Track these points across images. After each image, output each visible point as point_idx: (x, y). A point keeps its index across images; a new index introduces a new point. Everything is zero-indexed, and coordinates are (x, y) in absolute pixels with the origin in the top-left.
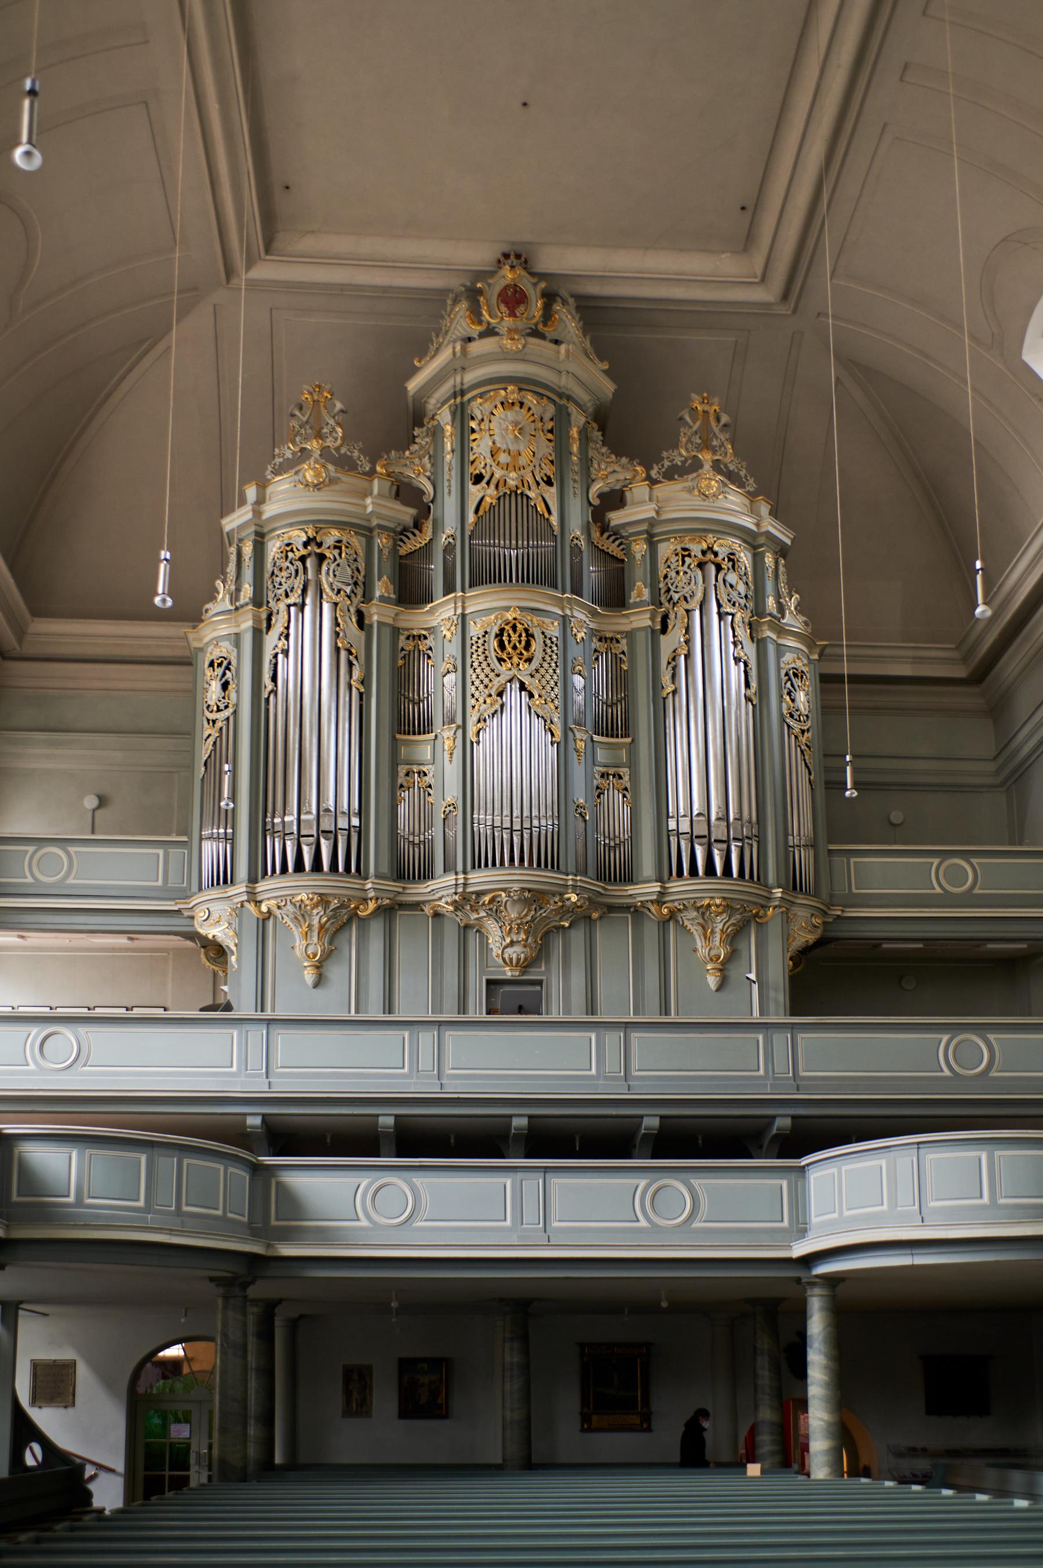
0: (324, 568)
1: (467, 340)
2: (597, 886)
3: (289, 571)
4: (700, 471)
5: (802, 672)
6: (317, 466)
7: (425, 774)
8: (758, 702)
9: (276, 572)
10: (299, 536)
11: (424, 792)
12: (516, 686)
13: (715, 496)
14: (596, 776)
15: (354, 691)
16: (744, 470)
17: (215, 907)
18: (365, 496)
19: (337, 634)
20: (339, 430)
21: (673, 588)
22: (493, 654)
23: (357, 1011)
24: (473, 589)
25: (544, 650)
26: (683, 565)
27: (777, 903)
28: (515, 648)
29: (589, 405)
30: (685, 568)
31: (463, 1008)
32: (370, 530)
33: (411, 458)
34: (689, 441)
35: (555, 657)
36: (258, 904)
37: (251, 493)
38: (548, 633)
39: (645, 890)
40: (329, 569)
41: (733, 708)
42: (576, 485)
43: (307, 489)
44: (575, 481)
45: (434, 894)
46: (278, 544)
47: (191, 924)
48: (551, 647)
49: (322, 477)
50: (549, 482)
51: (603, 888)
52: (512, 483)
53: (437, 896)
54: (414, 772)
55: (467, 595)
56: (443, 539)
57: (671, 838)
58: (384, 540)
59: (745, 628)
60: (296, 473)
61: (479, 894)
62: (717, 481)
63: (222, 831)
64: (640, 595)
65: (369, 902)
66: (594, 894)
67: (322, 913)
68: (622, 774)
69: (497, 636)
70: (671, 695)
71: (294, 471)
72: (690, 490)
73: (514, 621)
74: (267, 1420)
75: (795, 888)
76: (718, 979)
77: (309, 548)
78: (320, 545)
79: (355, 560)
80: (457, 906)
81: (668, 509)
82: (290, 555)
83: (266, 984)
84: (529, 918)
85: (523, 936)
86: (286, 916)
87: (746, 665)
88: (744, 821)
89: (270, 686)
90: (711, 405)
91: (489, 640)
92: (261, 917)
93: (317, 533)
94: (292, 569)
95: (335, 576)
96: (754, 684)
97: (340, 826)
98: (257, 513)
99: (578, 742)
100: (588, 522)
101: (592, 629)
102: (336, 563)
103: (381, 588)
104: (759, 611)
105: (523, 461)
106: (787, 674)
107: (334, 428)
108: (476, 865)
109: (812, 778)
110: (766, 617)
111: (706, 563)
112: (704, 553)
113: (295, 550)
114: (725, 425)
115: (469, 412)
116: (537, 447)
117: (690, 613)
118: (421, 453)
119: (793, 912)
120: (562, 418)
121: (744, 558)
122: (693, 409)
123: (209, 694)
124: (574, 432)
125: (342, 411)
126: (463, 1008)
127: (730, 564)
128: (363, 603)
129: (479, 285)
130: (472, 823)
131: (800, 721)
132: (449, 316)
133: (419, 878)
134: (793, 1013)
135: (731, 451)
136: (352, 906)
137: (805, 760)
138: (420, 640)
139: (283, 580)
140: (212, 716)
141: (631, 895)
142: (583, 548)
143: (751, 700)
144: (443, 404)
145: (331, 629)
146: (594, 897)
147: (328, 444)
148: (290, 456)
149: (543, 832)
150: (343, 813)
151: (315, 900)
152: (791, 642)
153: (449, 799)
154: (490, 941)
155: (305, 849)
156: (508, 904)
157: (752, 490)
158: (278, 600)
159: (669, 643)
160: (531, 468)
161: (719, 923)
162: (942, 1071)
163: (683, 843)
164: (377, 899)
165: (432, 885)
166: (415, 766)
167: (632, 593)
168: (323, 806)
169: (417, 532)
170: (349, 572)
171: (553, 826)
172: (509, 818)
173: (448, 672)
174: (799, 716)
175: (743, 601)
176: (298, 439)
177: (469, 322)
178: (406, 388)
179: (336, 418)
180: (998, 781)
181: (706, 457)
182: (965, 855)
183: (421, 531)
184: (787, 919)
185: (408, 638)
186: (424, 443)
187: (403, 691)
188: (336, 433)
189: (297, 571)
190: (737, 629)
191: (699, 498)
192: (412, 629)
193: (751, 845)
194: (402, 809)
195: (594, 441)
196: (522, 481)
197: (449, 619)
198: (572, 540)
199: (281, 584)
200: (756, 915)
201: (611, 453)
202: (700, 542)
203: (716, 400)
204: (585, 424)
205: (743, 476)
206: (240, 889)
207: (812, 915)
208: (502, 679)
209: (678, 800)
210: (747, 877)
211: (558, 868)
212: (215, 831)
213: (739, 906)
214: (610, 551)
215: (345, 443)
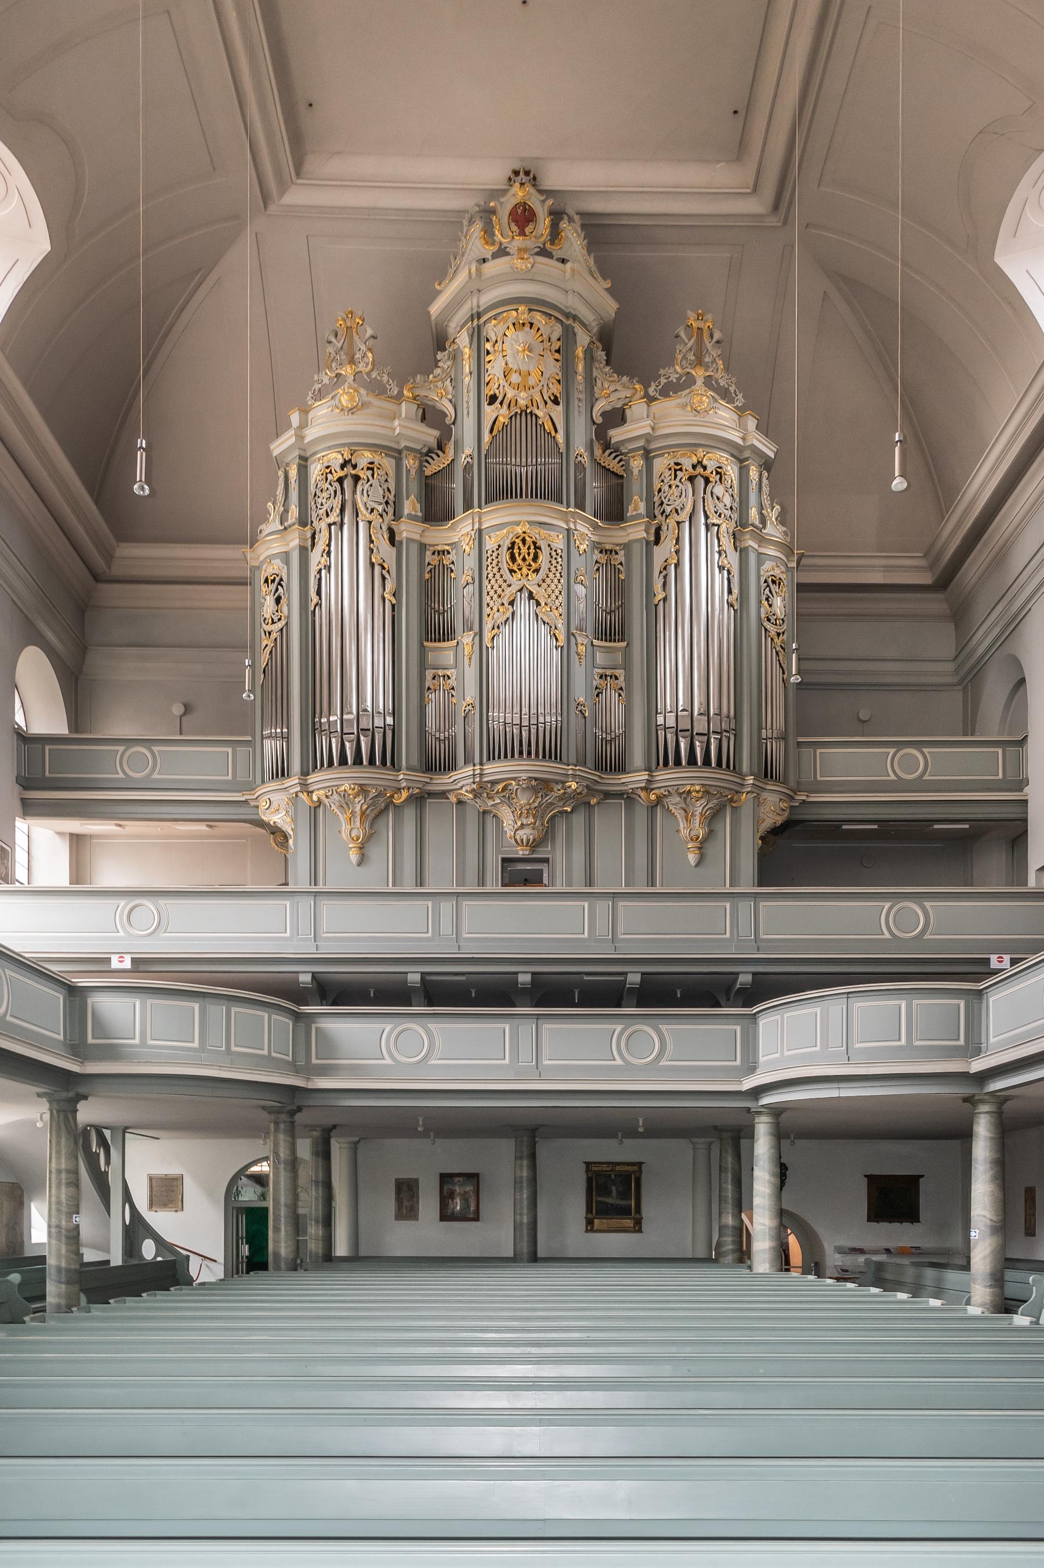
0: (359, 488)
1: (482, 261)
2: (594, 775)
3: (328, 492)
4: (693, 387)
5: (780, 579)
6: (351, 391)
7: (449, 678)
8: (739, 608)
9: (317, 493)
10: (336, 459)
11: (448, 693)
12: (525, 595)
13: (706, 411)
14: (596, 678)
15: (387, 601)
16: (734, 386)
17: (276, 797)
18: (394, 419)
19: (372, 551)
20: (370, 355)
21: (666, 501)
22: (505, 566)
23: (394, 885)
24: (488, 505)
25: (550, 562)
26: (675, 479)
27: (749, 789)
28: (524, 559)
29: (594, 324)
30: (677, 482)
31: (482, 882)
32: (400, 452)
33: (435, 382)
34: (684, 357)
35: (559, 568)
36: (310, 794)
37: (295, 418)
38: (554, 546)
39: (635, 779)
40: (363, 490)
41: (717, 613)
42: (580, 404)
43: (342, 412)
44: (580, 400)
45: (456, 784)
46: (319, 467)
47: (256, 812)
48: (556, 559)
49: (356, 401)
50: (556, 402)
51: (600, 776)
52: (522, 403)
53: (460, 785)
54: (440, 677)
55: (483, 511)
56: (463, 460)
57: (659, 732)
58: (412, 462)
59: (729, 537)
60: (333, 398)
61: (494, 783)
62: (708, 397)
63: (279, 730)
64: (635, 510)
65: (402, 791)
66: (592, 783)
67: (363, 801)
68: (618, 675)
69: (509, 549)
70: (662, 602)
71: (331, 396)
72: (684, 406)
73: (524, 535)
74: (327, 1221)
75: (766, 776)
76: (697, 856)
77: (345, 469)
78: (355, 467)
79: (386, 481)
80: (476, 795)
81: (664, 424)
82: (329, 476)
83: (318, 864)
84: (536, 804)
85: (531, 820)
86: (333, 803)
87: (729, 573)
88: (723, 716)
89: (315, 599)
90: (705, 322)
91: (502, 553)
92: (313, 806)
93: (352, 455)
94: (332, 490)
95: (368, 496)
96: (736, 591)
97: (376, 725)
98: (300, 437)
99: (579, 645)
100: (592, 440)
101: (594, 542)
102: (369, 483)
103: (411, 506)
104: (743, 522)
105: (532, 381)
106: (766, 581)
107: (365, 353)
108: (491, 757)
109: (785, 677)
110: (748, 527)
111: (697, 476)
112: (694, 467)
113: (333, 471)
114: (718, 342)
115: (485, 334)
116: (545, 367)
117: (680, 525)
118: (443, 376)
119: (764, 798)
120: (568, 337)
121: (731, 471)
122: (688, 326)
123: (265, 608)
124: (580, 352)
125: (374, 337)
126: (482, 882)
127: (718, 476)
128: (394, 520)
129: (492, 204)
130: (488, 720)
131: (776, 625)
132: (465, 237)
133: (445, 770)
134: (760, 885)
135: (722, 367)
136: (388, 795)
137: (779, 660)
138: (444, 555)
139: (324, 501)
140: (268, 628)
141: (624, 783)
142: (586, 465)
143: (732, 606)
144: (462, 327)
145: (365, 546)
146: (591, 785)
147: (358, 370)
148: (328, 382)
149: (548, 728)
150: (380, 713)
151: (356, 790)
152: (771, 551)
153: (469, 699)
154: (504, 825)
155: (347, 744)
156: (518, 791)
157: (740, 405)
158: (320, 519)
159: (662, 553)
160: (539, 387)
161: (699, 807)
162: (883, 934)
163: (669, 736)
164: (409, 788)
165: (455, 775)
166: (440, 670)
167: (630, 507)
168: (362, 707)
169: (440, 453)
170: (382, 492)
171: (556, 721)
172: (518, 715)
173: (468, 584)
174: (776, 620)
175: (728, 513)
176: (333, 365)
177: (484, 242)
178: (429, 312)
179: (367, 343)
180: (954, 680)
181: (699, 374)
182: (918, 745)
183: (444, 453)
184: (758, 801)
185: (434, 553)
186: (446, 367)
187: (429, 602)
188: (368, 358)
189: (335, 492)
190: (722, 539)
191: (692, 414)
192: (437, 545)
193: (729, 738)
194: (430, 709)
195: (598, 361)
196: (532, 400)
197: (468, 534)
198: (576, 458)
199: (322, 505)
200: (731, 800)
201: (613, 372)
202: (690, 457)
203: (709, 316)
204: (589, 343)
205: (732, 392)
206: (293, 782)
207: (781, 799)
208: (514, 588)
209: (666, 700)
210: (724, 766)
211: (560, 760)
212: (273, 731)
213: (715, 793)
214: (610, 467)
215: (376, 367)
